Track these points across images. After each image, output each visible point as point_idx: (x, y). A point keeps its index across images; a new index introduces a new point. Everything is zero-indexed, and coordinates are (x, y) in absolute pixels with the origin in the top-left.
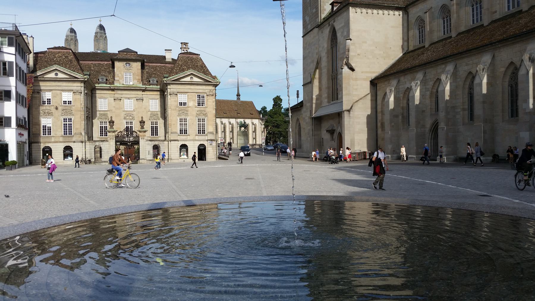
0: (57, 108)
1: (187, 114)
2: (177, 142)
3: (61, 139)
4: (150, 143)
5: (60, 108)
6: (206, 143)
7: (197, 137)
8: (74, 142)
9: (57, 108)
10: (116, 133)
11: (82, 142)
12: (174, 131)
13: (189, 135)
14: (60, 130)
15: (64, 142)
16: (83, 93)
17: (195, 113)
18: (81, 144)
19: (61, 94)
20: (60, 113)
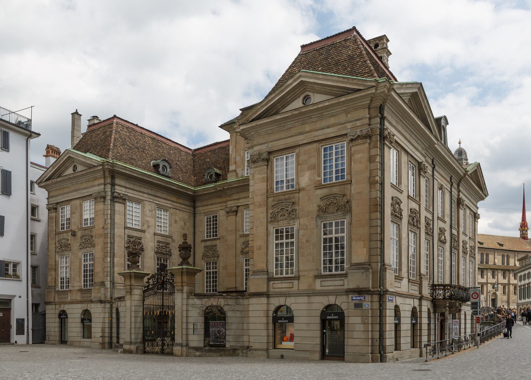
0: (74, 234)
1: (292, 215)
2: (264, 300)
3: (78, 297)
4: (197, 302)
5: (79, 234)
6: (344, 303)
7: (318, 281)
8: (91, 302)
9: (74, 234)
10: (146, 279)
11: (101, 302)
12: (261, 266)
13: (298, 278)
14: (78, 278)
15: (81, 302)
16: (109, 197)
17: (314, 208)
18: (99, 305)
19: (81, 205)
20: (79, 244)
